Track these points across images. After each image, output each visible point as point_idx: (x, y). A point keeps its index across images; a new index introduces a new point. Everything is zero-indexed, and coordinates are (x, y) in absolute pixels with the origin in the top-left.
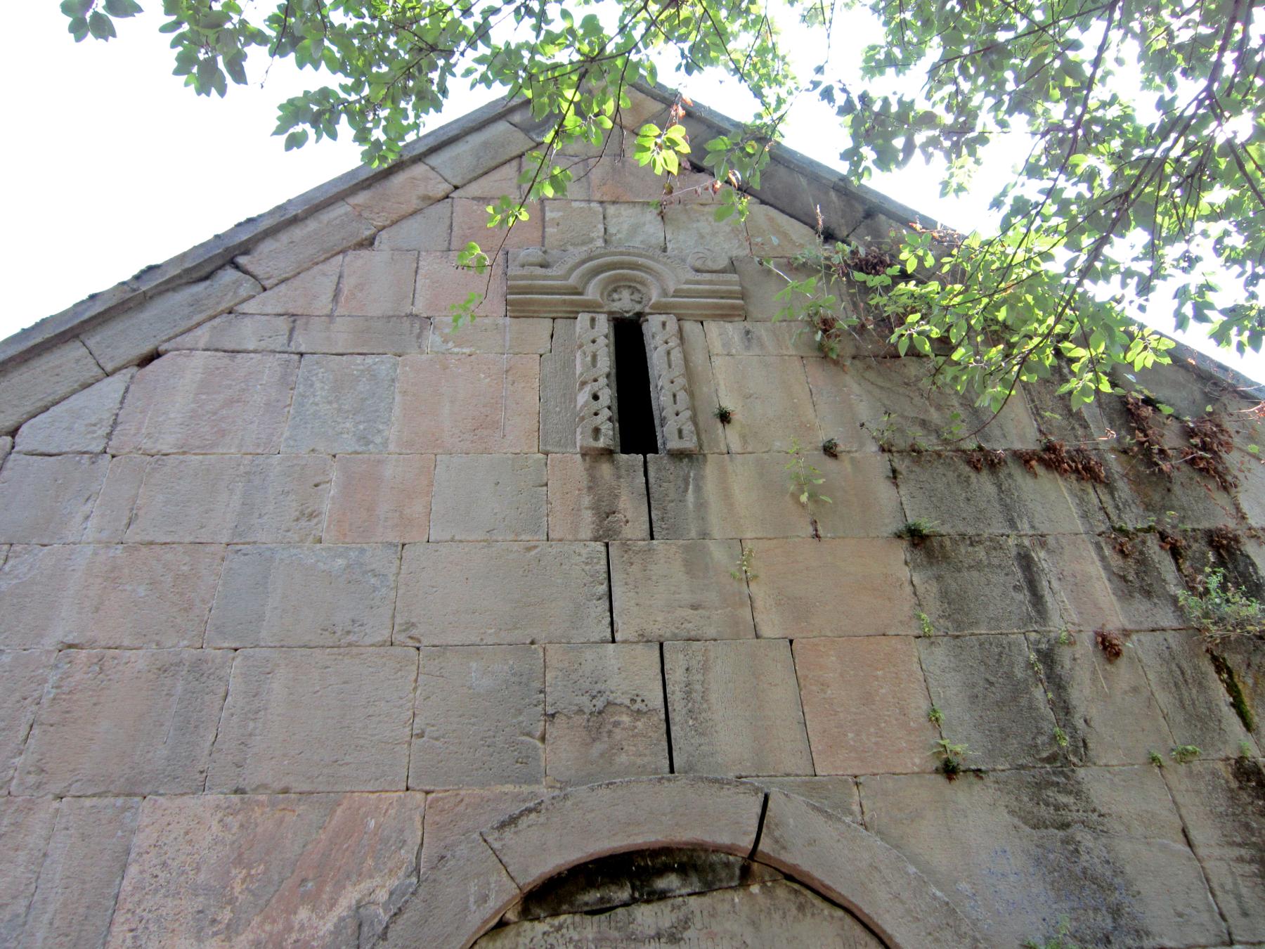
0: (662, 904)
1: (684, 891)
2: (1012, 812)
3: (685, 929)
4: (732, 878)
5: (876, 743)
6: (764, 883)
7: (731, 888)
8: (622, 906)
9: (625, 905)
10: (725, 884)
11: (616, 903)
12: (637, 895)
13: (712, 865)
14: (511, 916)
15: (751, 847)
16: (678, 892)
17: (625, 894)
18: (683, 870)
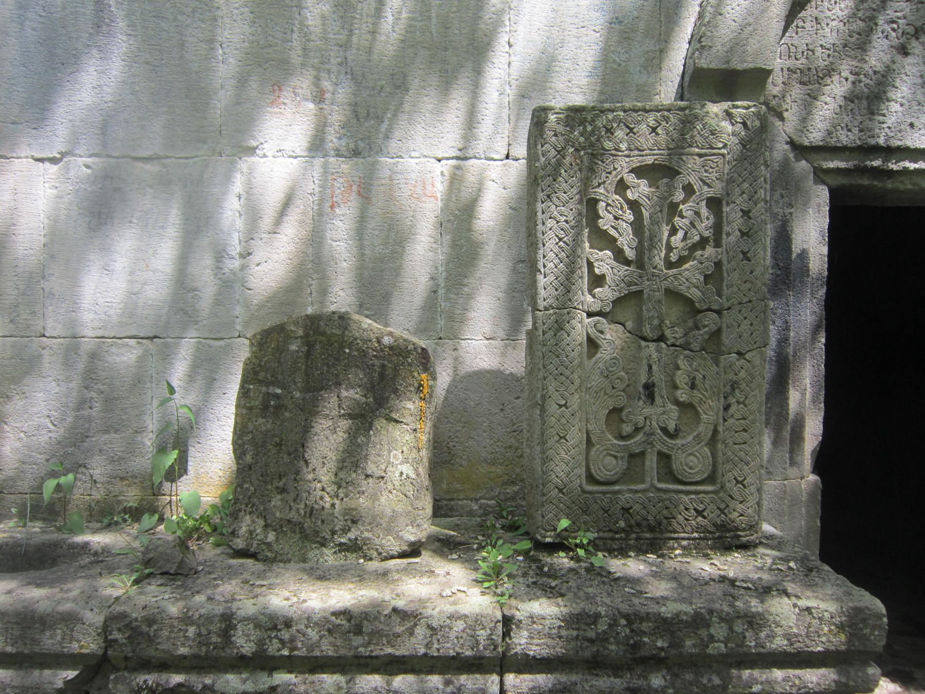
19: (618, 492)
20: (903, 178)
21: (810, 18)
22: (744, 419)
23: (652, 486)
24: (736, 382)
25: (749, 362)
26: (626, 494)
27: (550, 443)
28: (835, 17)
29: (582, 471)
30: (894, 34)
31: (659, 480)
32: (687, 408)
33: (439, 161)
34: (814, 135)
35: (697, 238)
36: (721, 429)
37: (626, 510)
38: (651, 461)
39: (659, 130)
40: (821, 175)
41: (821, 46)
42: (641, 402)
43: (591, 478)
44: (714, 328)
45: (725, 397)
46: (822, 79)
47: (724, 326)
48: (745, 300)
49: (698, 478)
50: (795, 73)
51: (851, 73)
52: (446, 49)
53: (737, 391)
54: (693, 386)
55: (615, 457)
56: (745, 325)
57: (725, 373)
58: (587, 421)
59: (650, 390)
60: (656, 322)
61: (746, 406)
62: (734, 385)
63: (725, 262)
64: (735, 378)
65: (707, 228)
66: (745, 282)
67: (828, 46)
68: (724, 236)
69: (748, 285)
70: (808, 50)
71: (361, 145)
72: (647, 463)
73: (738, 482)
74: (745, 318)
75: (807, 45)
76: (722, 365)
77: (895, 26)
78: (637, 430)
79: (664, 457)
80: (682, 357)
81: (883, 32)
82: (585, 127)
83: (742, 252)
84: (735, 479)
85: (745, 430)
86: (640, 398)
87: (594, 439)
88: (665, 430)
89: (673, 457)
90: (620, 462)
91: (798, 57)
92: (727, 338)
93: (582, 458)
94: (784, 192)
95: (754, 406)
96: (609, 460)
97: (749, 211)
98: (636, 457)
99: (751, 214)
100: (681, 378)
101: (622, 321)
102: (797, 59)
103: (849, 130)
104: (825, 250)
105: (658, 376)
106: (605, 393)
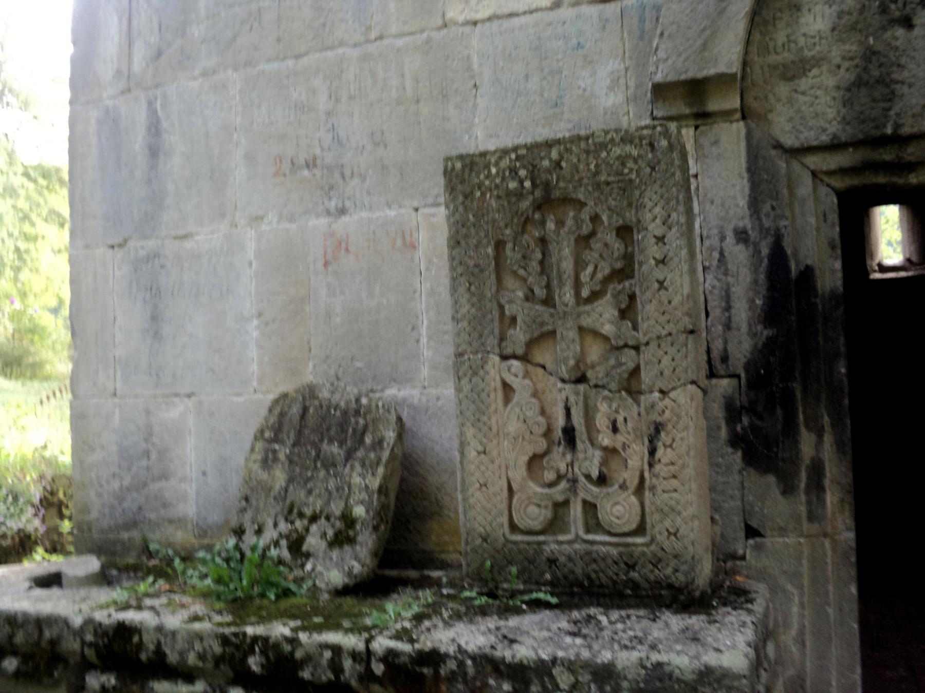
19: (544, 543)
22: (673, 464)
23: (577, 536)
24: (660, 424)
25: (674, 401)
26: (552, 545)
27: (471, 490)
29: (505, 520)
31: (588, 531)
32: (611, 452)
33: (417, 210)
34: (806, 134)
35: (607, 271)
36: (647, 475)
37: (552, 562)
38: (575, 510)
39: (563, 164)
40: (826, 179)
42: (561, 449)
43: (513, 527)
44: (631, 365)
45: (650, 441)
47: (642, 362)
48: (664, 333)
49: (626, 529)
52: (418, 101)
53: (663, 434)
54: (615, 430)
55: (539, 506)
56: (666, 360)
57: (648, 414)
58: (507, 468)
59: (569, 434)
60: (572, 362)
61: (673, 449)
62: (658, 428)
63: (638, 293)
64: (659, 419)
65: (618, 259)
66: (664, 313)
68: (636, 266)
69: (667, 317)
71: (348, 204)
72: (572, 512)
73: (669, 533)
74: (666, 353)
76: (642, 405)
78: (560, 477)
79: (590, 507)
80: (600, 399)
82: (489, 171)
83: (658, 281)
84: (667, 530)
85: (674, 477)
86: (559, 443)
87: (515, 487)
88: (588, 477)
89: (598, 506)
90: (543, 511)
92: (646, 377)
93: (504, 506)
94: (774, 204)
95: (684, 449)
96: (533, 509)
97: (664, 237)
98: (561, 507)
99: (666, 240)
100: (602, 422)
101: (542, 362)
102: (776, 53)
103: (848, 124)
104: (838, 265)
105: (578, 420)
106: (523, 438)
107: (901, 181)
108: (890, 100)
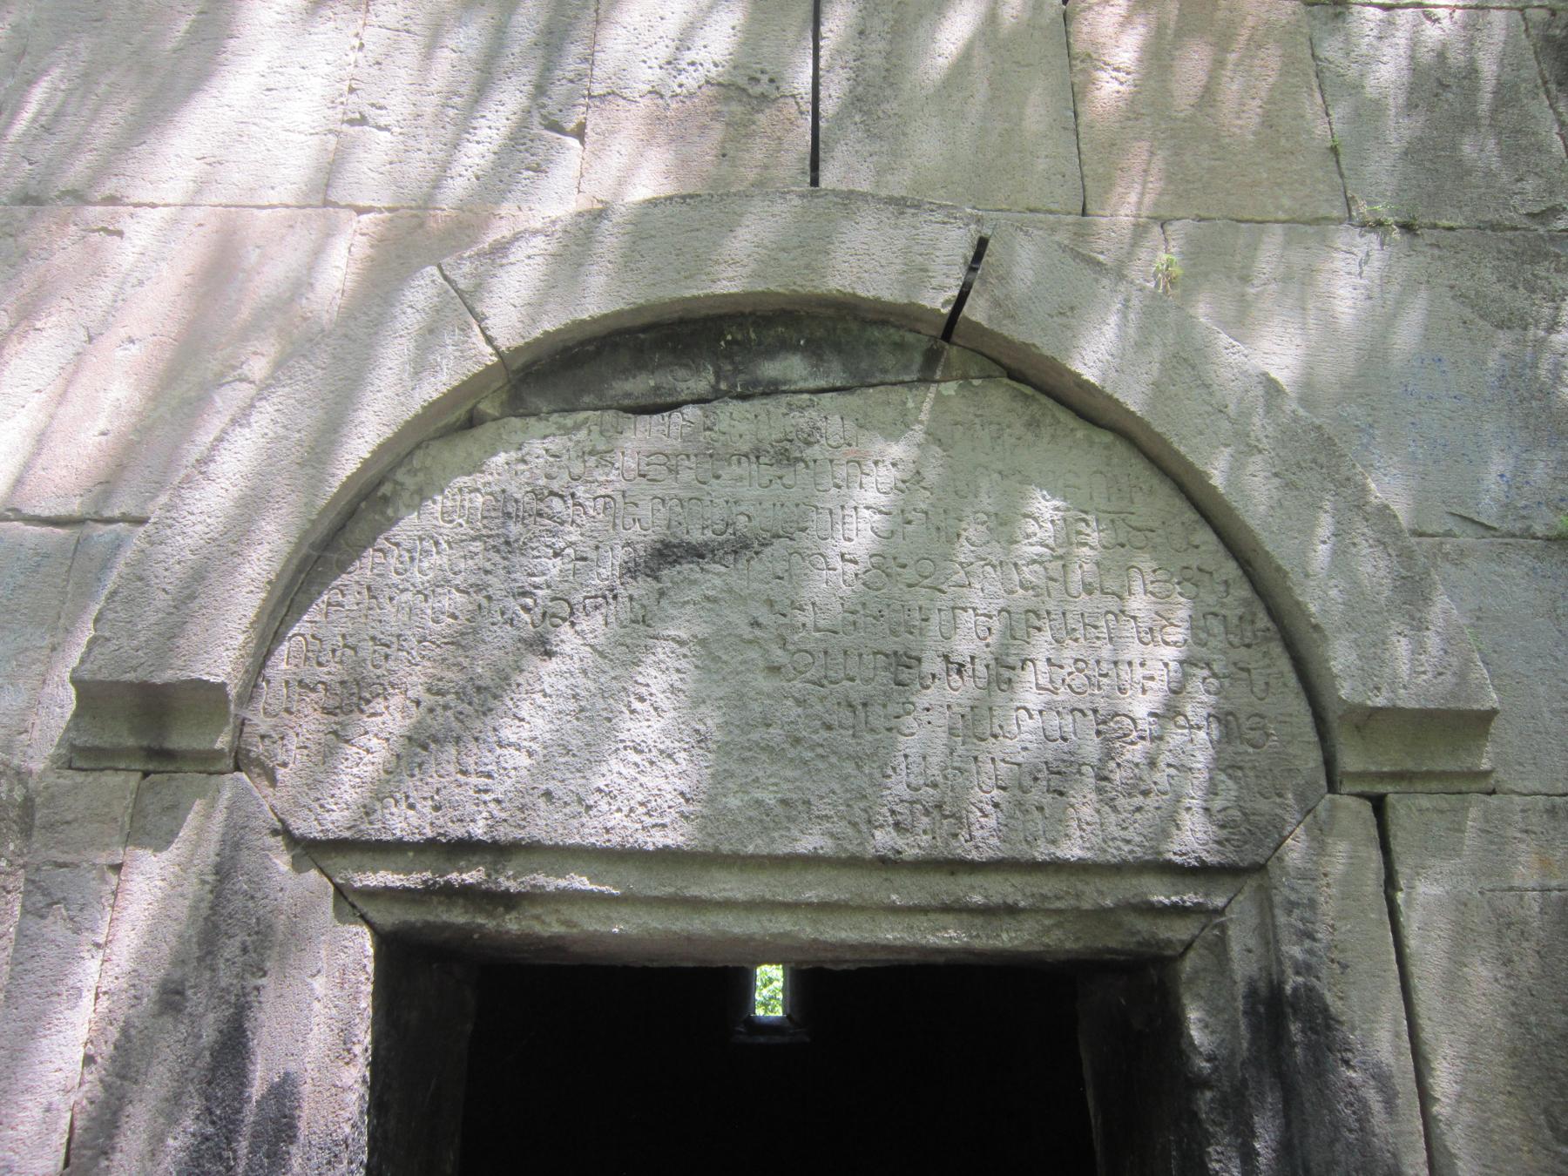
0: (770, 403)
1: (812, 384)
2: (1461, 297)
3: (809, 444)
4: (906, 368)
5: (1211, 170)
6: (965, 377)
7: (902, 383)
8: (694, 402)
9: (699, 401)
10: (891, 378)
11: (683, 397)
12: (723, 386)
13: (871, 345)
14: (487, 407)
15: (946, 310)
16: (801, 385)
17: (701, 383)
18: (814, 351)
20: (538, 910)
21: (356, 587)
28: (408, 585)
30: (526, 617)
34: (335, 816)
41: (373, 638)
46: (368, 702)
50: (314, 690)
51: (429, 690)
67: (386, 639)
70: (346, 646)
75: (344, 636)
77: (529, 601)
81: (503, 614)
91: (323, 659)
102: (320, 664)
103: (411, 807)
107: (490, 924)
108: (489, 776)
